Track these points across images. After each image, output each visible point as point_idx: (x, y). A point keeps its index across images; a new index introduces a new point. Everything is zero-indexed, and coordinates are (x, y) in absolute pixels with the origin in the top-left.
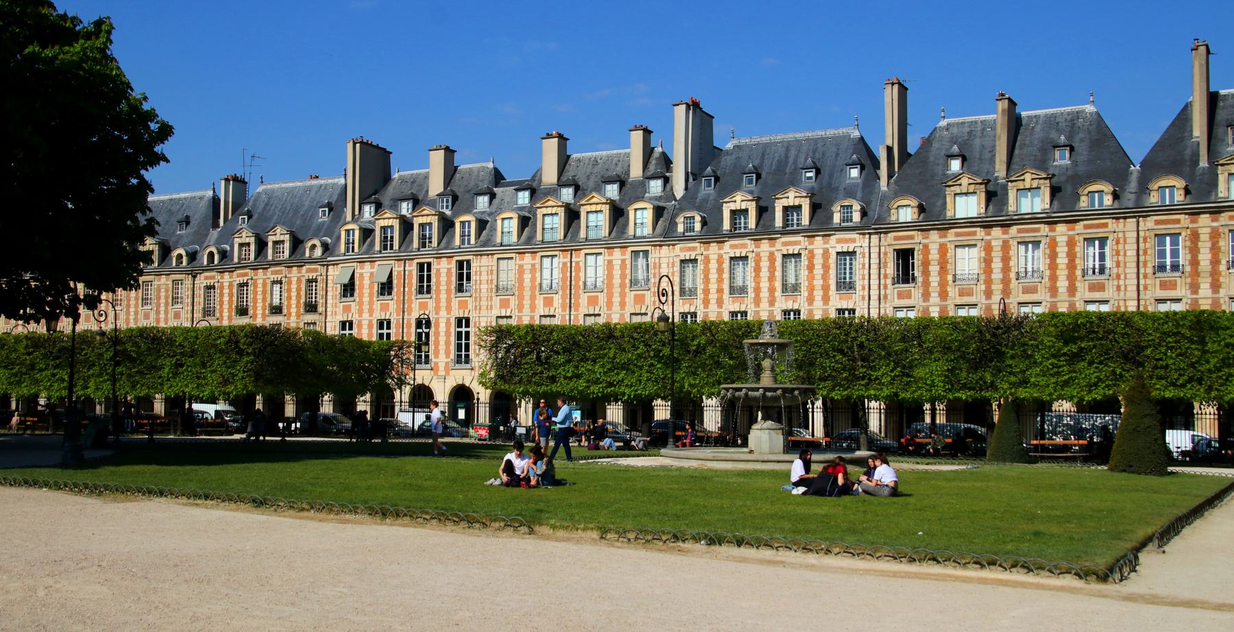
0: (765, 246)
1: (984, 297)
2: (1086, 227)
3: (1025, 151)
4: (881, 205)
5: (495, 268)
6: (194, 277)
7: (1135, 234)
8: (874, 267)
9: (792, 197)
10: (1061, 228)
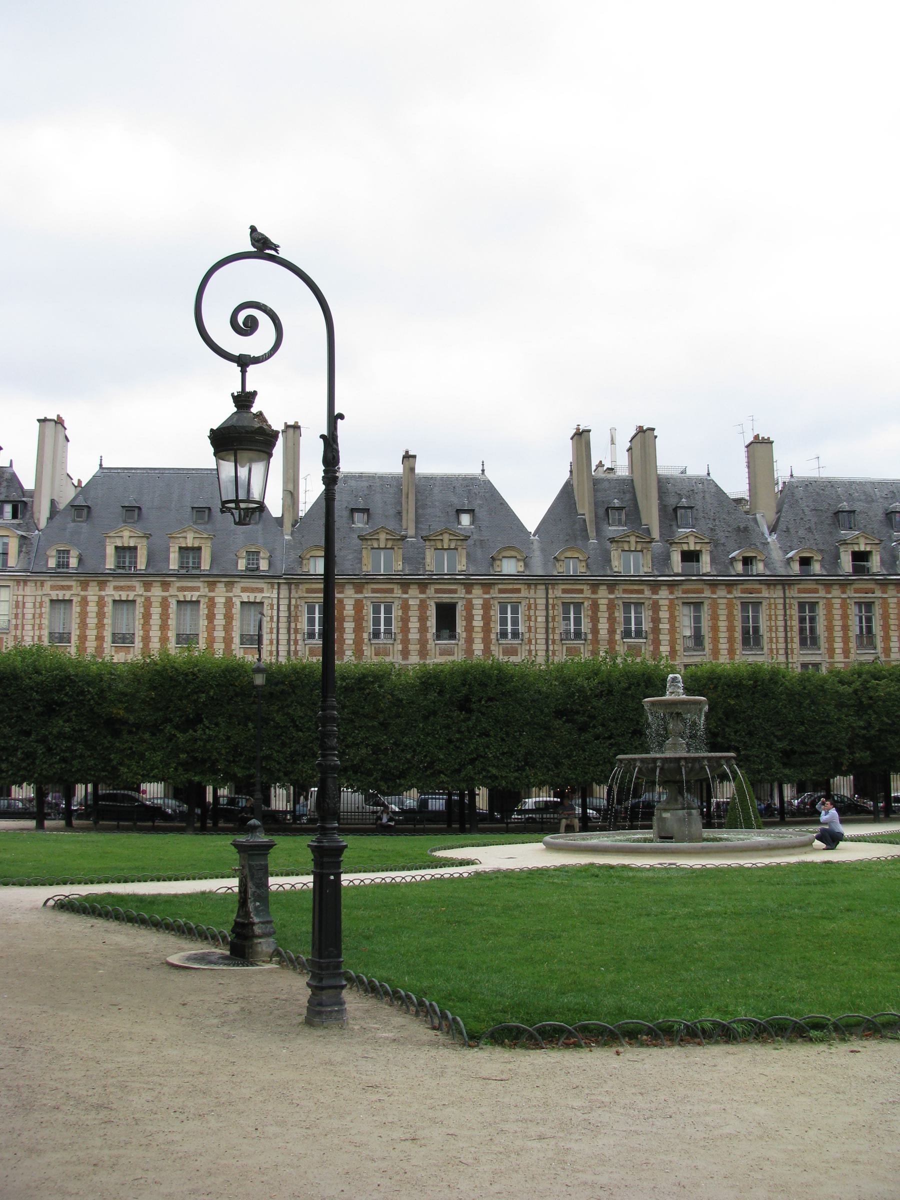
1: (400, 657)
7: (544, 601)
8: (283, 620)
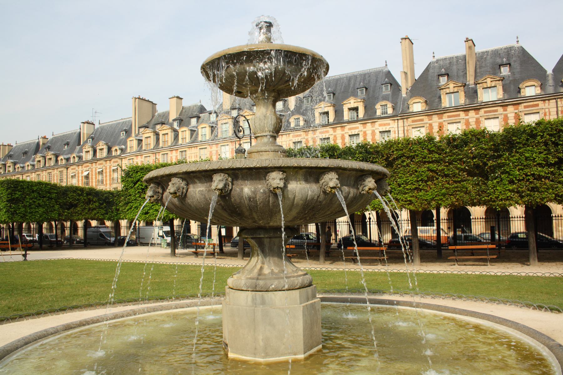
0: (339, 131)
2: (525, 107)
3: (483, 69)
4: (403, 104)
5: (198, 154)
6: (67, 169)
7: (555, 109)
9: (352, 102)
10: (510, 109)
